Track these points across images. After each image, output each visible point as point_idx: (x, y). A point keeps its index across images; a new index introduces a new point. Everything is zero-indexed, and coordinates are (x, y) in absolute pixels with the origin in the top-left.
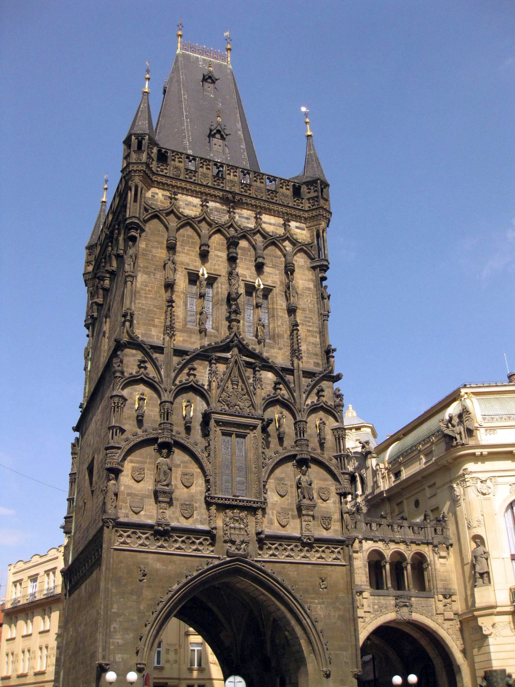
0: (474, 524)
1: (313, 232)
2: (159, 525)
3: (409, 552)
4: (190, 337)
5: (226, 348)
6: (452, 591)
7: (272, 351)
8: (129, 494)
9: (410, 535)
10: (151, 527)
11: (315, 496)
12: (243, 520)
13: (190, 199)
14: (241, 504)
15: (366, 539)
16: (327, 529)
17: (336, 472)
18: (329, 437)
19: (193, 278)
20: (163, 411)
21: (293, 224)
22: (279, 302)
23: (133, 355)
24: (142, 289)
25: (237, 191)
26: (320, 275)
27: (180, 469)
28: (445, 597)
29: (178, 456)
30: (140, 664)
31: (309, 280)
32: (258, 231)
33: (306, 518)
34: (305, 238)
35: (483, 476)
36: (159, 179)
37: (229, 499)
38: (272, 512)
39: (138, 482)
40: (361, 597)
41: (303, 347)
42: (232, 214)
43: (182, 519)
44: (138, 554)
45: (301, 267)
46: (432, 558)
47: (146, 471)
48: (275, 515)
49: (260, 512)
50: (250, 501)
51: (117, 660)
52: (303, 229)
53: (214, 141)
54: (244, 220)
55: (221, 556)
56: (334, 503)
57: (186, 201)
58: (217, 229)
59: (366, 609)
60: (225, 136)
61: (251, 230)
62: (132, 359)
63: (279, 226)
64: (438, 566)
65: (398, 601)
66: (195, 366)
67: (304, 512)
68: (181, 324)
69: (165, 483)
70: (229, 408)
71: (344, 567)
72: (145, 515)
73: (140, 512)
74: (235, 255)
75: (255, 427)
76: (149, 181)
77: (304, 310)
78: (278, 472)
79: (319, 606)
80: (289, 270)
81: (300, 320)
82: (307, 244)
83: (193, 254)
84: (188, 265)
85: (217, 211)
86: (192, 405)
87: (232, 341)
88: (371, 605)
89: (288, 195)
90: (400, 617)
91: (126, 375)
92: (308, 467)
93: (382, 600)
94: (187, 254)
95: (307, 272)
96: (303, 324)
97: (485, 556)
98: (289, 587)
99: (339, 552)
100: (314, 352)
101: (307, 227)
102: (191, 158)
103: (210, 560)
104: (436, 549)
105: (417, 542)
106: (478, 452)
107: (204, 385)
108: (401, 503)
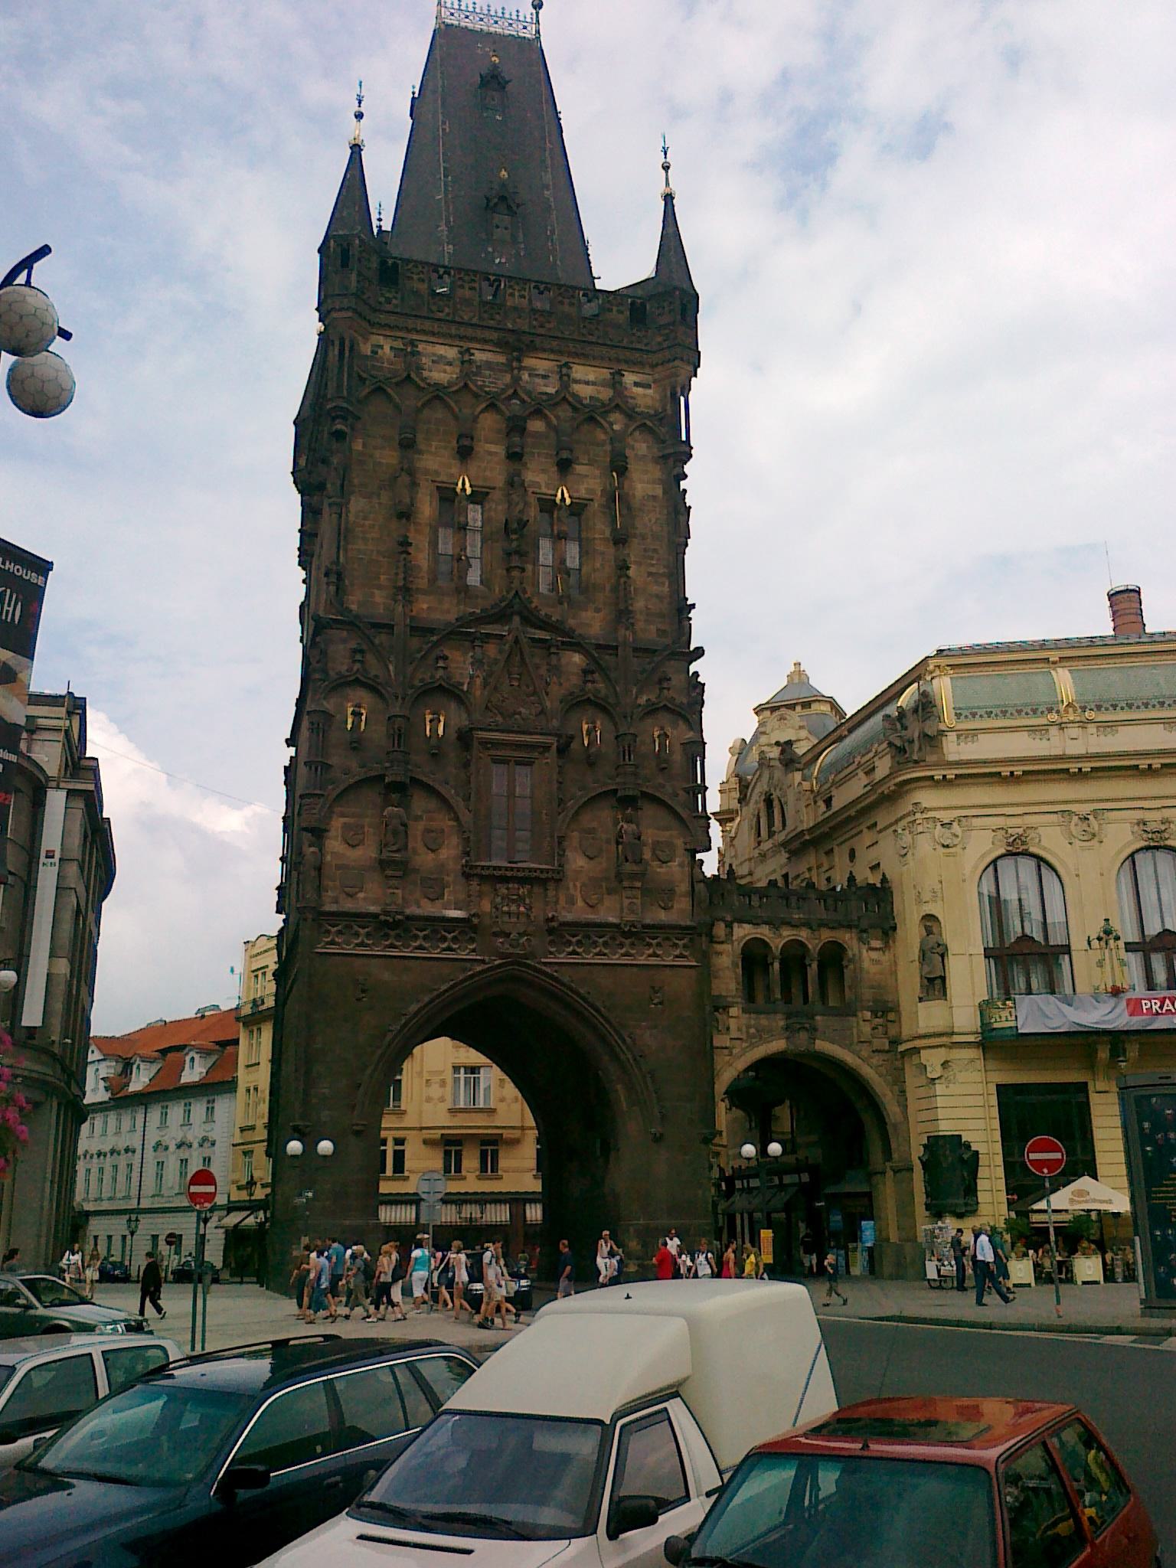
0: (926, 896)
1: (665, 390)
2: (386, 913)
3: (814, 941)
5: (500, 616)
6: (890, 1005)
7: (584, 614)
8: (338, 867)
9: (820, 912)
10: (376, 916)
11: (647, 855)
13: (441, 350)
14: (520, 874)
15: (741, 921)
17: (684, 816)
18: (678, 757)
19: (447, 495)
20: (392, 732)
21: (629, 378)
22: (599, 526)
23: (344, 641)
25: (526, 328)
26: (675, 472)
28: (875, 1014)
29: (420, 803)
30: (357, 1125)
31: (654, 482)
32: (564, 398)
33: (629, 893)
34: (650, 402)
35: (946, 816)
36: (383, 318)
37: (500, 868)
38: (575, 886)
39: (353, 846)
40: (725, 1017)
41: (639, 604)
42: (516, 372)
43: (425, 902)
44: (354, 958)
46: (856, 951)
49: (551, 886)
50: (535, 870)
51: (323, 1119)
52: (649, 386)
53: (497, 218)
54: (538, 380)
55: (487, 958)
56: (681, 865)
57: (434, 355)
59: (734, 1034)
60: (515, 208)
62: (341, 647)
64: (866, 964)
65: (791, 1021)
66: (447, 652)
67: (626, 884)
69: (394, 848)
70: (504, 719)
71: (693, 972)
72: (365, 899)
73: (356, 893)
74: (518, 450)
75: (547, 748)
76: (365, 324)
77: (643, 537)
78: (587, 820)
79: (648, 1033)
80: (619, 466)
84: (437, 473)
86: (442, 719)
87: (510, 605)
88: (744, 1029)
90: (792, 1047)
91: (331, 673)
92: (636, 809)
93: (764, 1021)
95: (651, 467)
96: (639, 564)
97: (938, 950)
98: (598, 1004)
99: (685, 946)
102: (441, 271)
103: (468, 965)
104: (865, 935)
105: (831, 925)
106: (938, 774)
107: (463, 684)
108: (832, 850)
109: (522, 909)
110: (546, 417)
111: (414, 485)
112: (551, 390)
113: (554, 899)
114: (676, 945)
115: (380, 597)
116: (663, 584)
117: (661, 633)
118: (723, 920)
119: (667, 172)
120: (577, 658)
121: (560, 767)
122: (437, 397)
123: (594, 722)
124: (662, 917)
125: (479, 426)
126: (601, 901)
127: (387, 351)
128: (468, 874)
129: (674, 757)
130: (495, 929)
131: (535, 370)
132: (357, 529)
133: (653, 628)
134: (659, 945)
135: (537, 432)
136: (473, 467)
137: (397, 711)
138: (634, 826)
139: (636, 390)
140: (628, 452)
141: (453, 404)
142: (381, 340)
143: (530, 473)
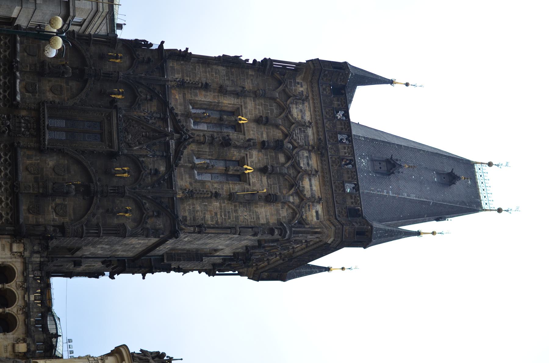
4: (181, 105)
7: (187, 176)
10: (15, 58)
11: (58, 201)
12: (28, 131)
16: (29, 210)
17: (83, 219)
18: (116, 221)
21: (319, 208)
24: (212, 69)
27: (65, 85)
31: (267, 219)
34: (310, 218)
38: (38, 160)
45: (277, 211)
47: (59, 59)
48: (36, 162)
56: (54, 220)
57: (305, 110)
58: (287, 133)
60: (391, 171)
61: (299, 164)
63: (312, 193)
68: (191, 99)
69: (51, 66)
73: (26, 52)
75: (111, 147)
76: (310, 79)
77: (236, 211)
80: (270, 199)
81: (225, 206)
82: (302, 217)
83: (257, 112)
84: (246, 108)
85: (305, 137)
86: (120, 97)
89: (346, 202)
94: (255, 108)
95: (275, 217)
96: (221, 208)
100: (197, 218)
101: (320, 221)
105: (26, 320)
109: (23, 130)
110: (287, 161)
111: (236, 95)
112: (302, 165)
113: (29, 146)
114: (8, 214)
115: (178, 76)
116: (212, 221)
117: (185, 219)
118: (25, 249)
119: (431, 233)
120: (162, 169)
121: (102, 153)
122: (284, 110)
123: (128, 172)
124: (23, 207)
125: (275, 130)
126: (30, 173)
127: (301, 89)
128: (41, 104)
129: (115, 220)
130: (11, 116)
131: (310, 159)
132: (210, 69)
133: (187, 214)
134: (7, 204)
135: (279, 158)
136: (253, 125)
137: (121, 74)
138: (74, 193)
139: (314, 211)
140: (280, 205)
141: (282, 116)
142: (305, 87)
143: (257, 153)
